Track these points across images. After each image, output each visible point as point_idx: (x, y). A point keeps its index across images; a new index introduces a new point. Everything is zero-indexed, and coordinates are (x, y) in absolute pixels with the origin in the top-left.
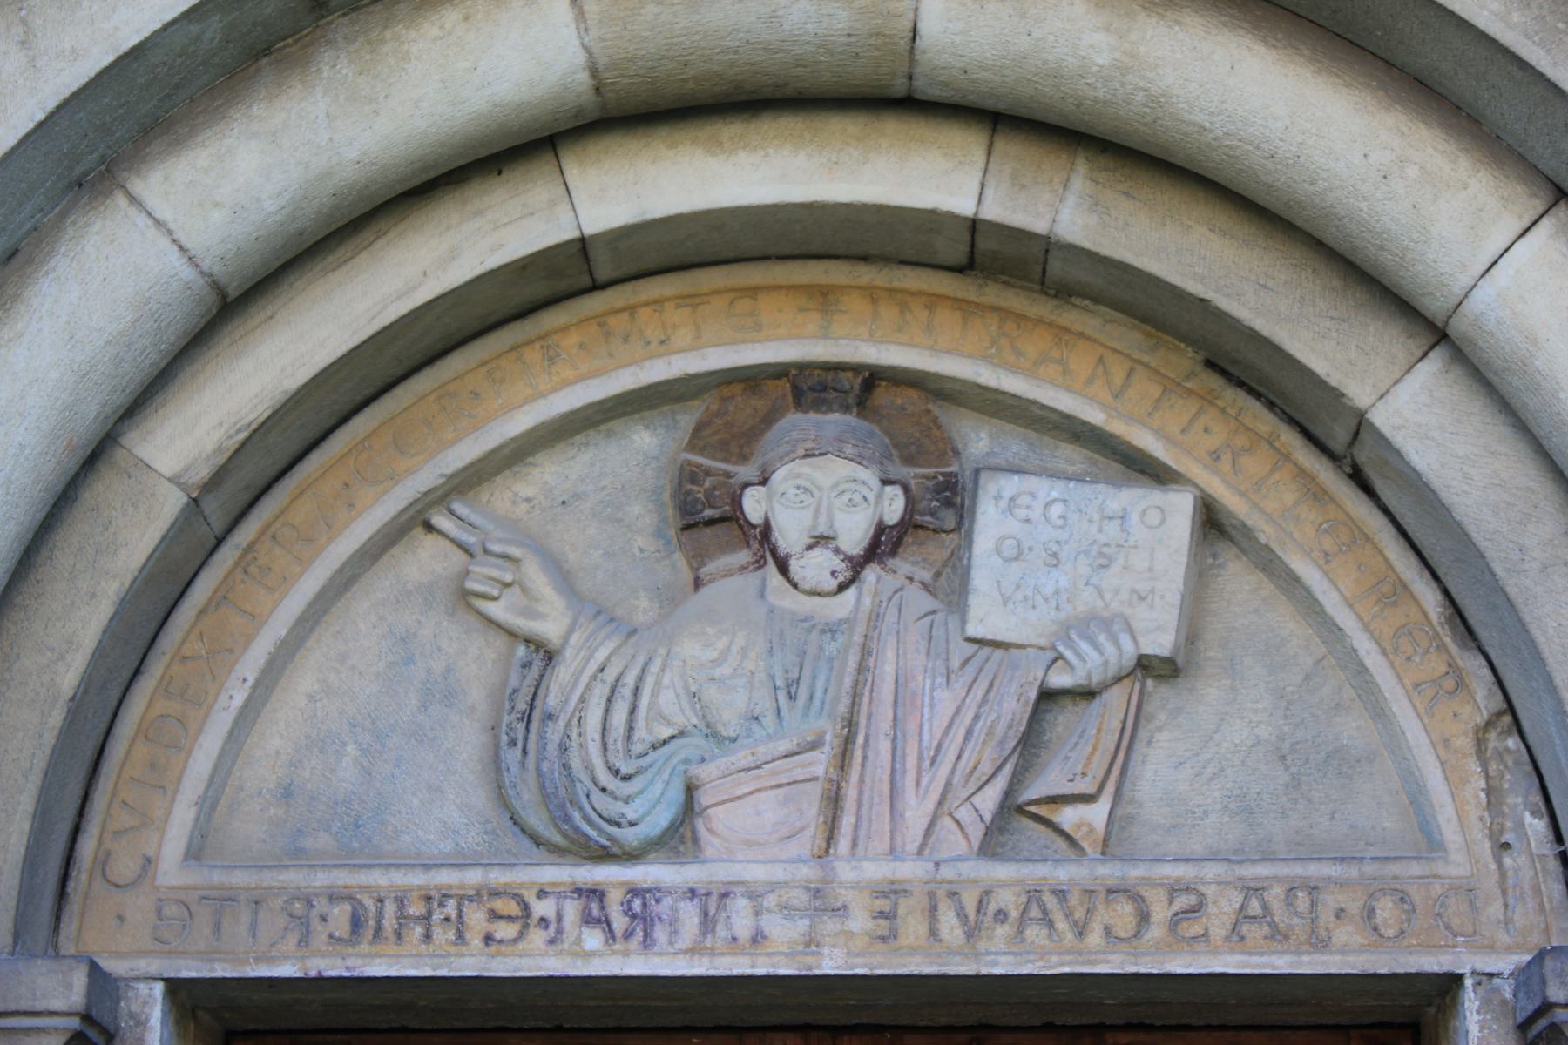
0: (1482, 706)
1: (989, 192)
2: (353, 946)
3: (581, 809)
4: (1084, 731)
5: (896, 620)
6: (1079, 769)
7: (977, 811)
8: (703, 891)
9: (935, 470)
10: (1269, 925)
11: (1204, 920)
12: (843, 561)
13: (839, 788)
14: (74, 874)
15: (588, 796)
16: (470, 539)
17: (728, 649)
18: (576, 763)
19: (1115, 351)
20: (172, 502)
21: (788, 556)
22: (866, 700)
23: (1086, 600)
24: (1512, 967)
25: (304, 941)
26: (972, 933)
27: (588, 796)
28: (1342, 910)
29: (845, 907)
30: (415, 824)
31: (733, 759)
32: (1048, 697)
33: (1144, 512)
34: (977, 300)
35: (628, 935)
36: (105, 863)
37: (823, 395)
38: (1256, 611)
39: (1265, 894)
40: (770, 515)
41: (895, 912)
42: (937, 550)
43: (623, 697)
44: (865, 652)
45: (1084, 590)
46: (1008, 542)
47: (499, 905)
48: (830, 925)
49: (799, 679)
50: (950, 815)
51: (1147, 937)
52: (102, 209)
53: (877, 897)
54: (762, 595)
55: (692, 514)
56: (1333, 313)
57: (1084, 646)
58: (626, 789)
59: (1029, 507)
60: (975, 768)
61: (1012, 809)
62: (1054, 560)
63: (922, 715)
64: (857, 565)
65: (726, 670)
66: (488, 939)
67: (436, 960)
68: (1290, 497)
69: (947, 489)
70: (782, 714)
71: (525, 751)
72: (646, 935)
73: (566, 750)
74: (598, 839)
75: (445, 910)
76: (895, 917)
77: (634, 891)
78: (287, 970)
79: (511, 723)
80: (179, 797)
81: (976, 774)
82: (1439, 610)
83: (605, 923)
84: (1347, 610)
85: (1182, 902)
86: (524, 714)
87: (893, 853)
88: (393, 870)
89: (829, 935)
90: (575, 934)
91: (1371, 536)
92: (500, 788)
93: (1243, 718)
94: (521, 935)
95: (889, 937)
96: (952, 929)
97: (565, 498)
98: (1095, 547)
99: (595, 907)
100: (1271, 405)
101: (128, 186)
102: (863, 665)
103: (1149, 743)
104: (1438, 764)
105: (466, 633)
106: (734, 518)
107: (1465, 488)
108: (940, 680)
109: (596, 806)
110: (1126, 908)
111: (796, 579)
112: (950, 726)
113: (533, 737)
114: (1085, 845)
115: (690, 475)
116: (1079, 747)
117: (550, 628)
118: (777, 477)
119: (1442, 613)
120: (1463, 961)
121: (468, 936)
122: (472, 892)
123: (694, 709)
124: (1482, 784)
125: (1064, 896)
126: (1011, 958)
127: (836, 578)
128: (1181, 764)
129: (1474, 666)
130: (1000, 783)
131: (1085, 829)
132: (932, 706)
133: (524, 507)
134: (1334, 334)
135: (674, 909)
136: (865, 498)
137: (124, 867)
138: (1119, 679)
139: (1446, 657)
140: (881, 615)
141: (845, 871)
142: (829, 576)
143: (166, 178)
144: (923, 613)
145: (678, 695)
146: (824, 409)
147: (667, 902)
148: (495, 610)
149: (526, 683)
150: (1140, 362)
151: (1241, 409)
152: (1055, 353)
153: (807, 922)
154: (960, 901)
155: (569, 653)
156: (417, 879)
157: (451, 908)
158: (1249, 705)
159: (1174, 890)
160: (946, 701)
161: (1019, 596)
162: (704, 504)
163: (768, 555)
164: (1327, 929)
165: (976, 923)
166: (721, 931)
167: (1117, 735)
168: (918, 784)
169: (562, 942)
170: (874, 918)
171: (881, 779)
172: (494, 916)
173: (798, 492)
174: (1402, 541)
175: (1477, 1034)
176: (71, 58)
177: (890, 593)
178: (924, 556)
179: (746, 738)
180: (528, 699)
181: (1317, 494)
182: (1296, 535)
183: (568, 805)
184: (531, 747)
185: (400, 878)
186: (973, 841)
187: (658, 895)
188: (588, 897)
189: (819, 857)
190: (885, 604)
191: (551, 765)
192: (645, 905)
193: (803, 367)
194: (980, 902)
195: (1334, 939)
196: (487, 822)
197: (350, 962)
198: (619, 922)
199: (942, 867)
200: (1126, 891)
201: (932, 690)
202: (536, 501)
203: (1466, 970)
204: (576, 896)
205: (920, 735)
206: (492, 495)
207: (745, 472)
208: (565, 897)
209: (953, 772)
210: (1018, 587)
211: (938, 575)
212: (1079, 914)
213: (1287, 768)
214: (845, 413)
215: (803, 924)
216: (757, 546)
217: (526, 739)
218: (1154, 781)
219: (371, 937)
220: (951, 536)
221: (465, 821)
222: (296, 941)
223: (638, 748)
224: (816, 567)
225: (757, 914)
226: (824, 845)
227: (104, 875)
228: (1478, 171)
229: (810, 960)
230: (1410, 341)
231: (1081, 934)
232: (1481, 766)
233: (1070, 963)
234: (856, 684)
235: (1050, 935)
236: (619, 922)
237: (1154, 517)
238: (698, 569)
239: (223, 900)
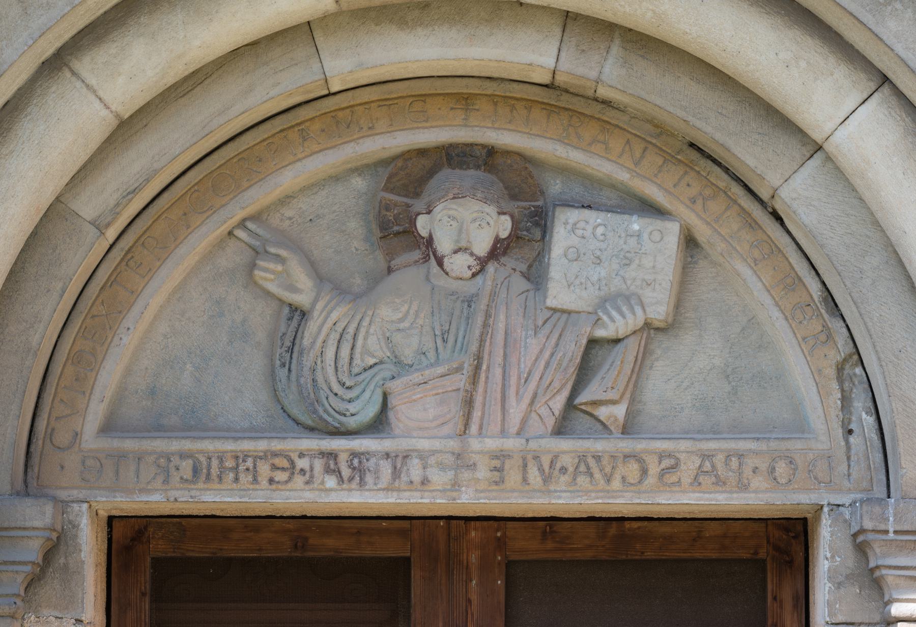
0: (841, 350)
1: (563, 54)
2: (194, 484)
3: (323, 405)
4: (613, 362)
5: (505, 296)
6: (610, 385)
7: (551, 409)
8: (394, 454)
9: (530, 203)
10: (716, 477)
11: (679, 473)
12: (475, 260)
13: (471, 395)
14: (34, 441)
15: (327, 398)
17: (408, 312)
19: (636, 135)
21: (443, 257)
22: (488, 344)
23: (616, 285)
24: (851, 501)
25: (166, 481)
26: (547, 479)
27: (327, 398)
28: (757, 468)
29: (475, 464)
30: (227, 411)
31: (410, 377)
32: (593, 343)
33: (651, 233)
34: (556, 104)
35: (351, 479)
36: (51, 435)
37: (464, 159)
38: (715, 290)
39: (714, 459)
40: (432, 232)
41: (503, 467)
43: (347, 340)
44: (488, 315)
45: (615, 279)
46: (571, 250)
48: (466, 475)
49: (449, 330)
50: (535, 411)
51: (646, 482)
52: (56, 78)
53: (493, 459)
54: (428, 279)
55: (386, 229)
56: (760, 130)
57: (614, 313)
59: (584, 229)
60: (550, 384)
61: (570, 405)
62: (598, 261)
63: (520, 353)
65: (406, 324)
66: (271, 481)
67: (242, 493)
68: (735, 226)
69: (536, 216)
70: (439, 351)
71: (290, 370)
72: (361, 479)
73: (314, 370)
74: (333, 423)
75: (246, 464)
76: (503, 470)
77: (354, 454)
79: (282, 354)
80: (93, 397)
81: (551, 388)
82: (819, 293)
83: (338, 473)
84: (766, 293)
85: (666, 463)
86: (289, 348)
87: (503, 433)
88: (216, 440)
89: (465, 481)
90: (321, 479)
91: (782, 249)
92: (275, 391)
93: (705, 353)
94: (290, 479)
95: (499, 482)
96: (535, 477)
97: (310, 218)
98: (622, 253)
99: (332, 463)
100: (727, 170)
101: (71, 64)
102: (486, 322)
103: (651, 368)
104: (814, 384)
105: (254, 299)
107: (832, 235)
108: (531, 332)
109: (332, 404)
111: (448, 270)
112: (536, 360)
113: (294, 361)
114: (612, 428)
116: (610, 372)
117: (302, 299)
118: (439, 210)
119: (821, 296)
120: (825, 498)
121: (259, 479)
122: (262, 454)
123: (388, 348)
124: (839, 396)
125: (600, 459)
126: (569, 494)
127: (471, 270)
128: (669, 380)
129: (836, 325)
130: (566, 393)
131: (612, 419)
132: (526, 347)
133: (288, 222)
134: (760, 143)
135: (377, 465)
136: (488, 223)
137: (63, 438)
138: (634, 332)
139: (822, 321)
140: (497, 292)
141: (475, 444)
142: (467, 269)
143: (92, 60)
144: (521, 291)
145: (379, 339)
146: (464, 167)
147: (373, 461)
149: (290, 330)
150: (651, 143)
151: (709, 172)
152: (600, 137)
153: (453, 472)
154: (540, 462)
155: (316, 314)
156: (230, 446)
157: (249, 463)
158: (710, 346)
159: (661, 456)
160: (534, 345)
161: (577, 282)
162: (393, 223)
163: (431, 253)
164: (748, 479)
165: (549, 474)
166: (404, 478)
167: (632, 365)
168: (517, 393)
169: (313, 483)
170: (491, 471)
171: (496, 391)
172: (274, 468)
173: (449, 220)
174: (799, 252)
175: (829, 538)
176: (47, 8)
177: (502, 280)
178: (522, 255)
179: (418, 365)
180: (292, 339)
181: (752, 224)
182: (738, 248)
183: (316, 403)
184: (293, 367)
186: (548, 427)
187: (368, 456)
188: (328, 457)
189: (460, 435)
190: (499, 286)
191: (306, 380)
192: (360, 462)
194: (552, 462)
195: (751, 485)
196: (268, 410)
197: (193, 493)
198: (346, 472)
199: (530, 442)
200: (635, 456)
201: (526, 338)
202: (295, 219)
203: (825, 503)
204: (321, 456)
205: (519, 365)
206: (269, 215)
207: (419, 205)
208: (315, 457)
209: (538, 387)
210: (577, 277)
211: (530, 266)
212: (608, 469)
213: (730, 383)
214: (477, 170)
215: (450, 474)
216: (424, 249)
217: (290, 363)
218: (653, 390)
219: (204, 479)
220: (538, 243)
221: (256, 409)
222: (161, 481)
223: (356, 370)
224: (460, 264)
225: (424, 468)
226: (463, 429)
227: (51, 442)
228: (840, 65)
229: (455, 494)
230: (803, 148)
231: (608, 481)
232: (839, 385)
233: (602, 498)
234: (482, 335)
235: (591, 481)
236: (346, 472)
237: (656, 236)
238: (390, 262)
239: (120, 457)
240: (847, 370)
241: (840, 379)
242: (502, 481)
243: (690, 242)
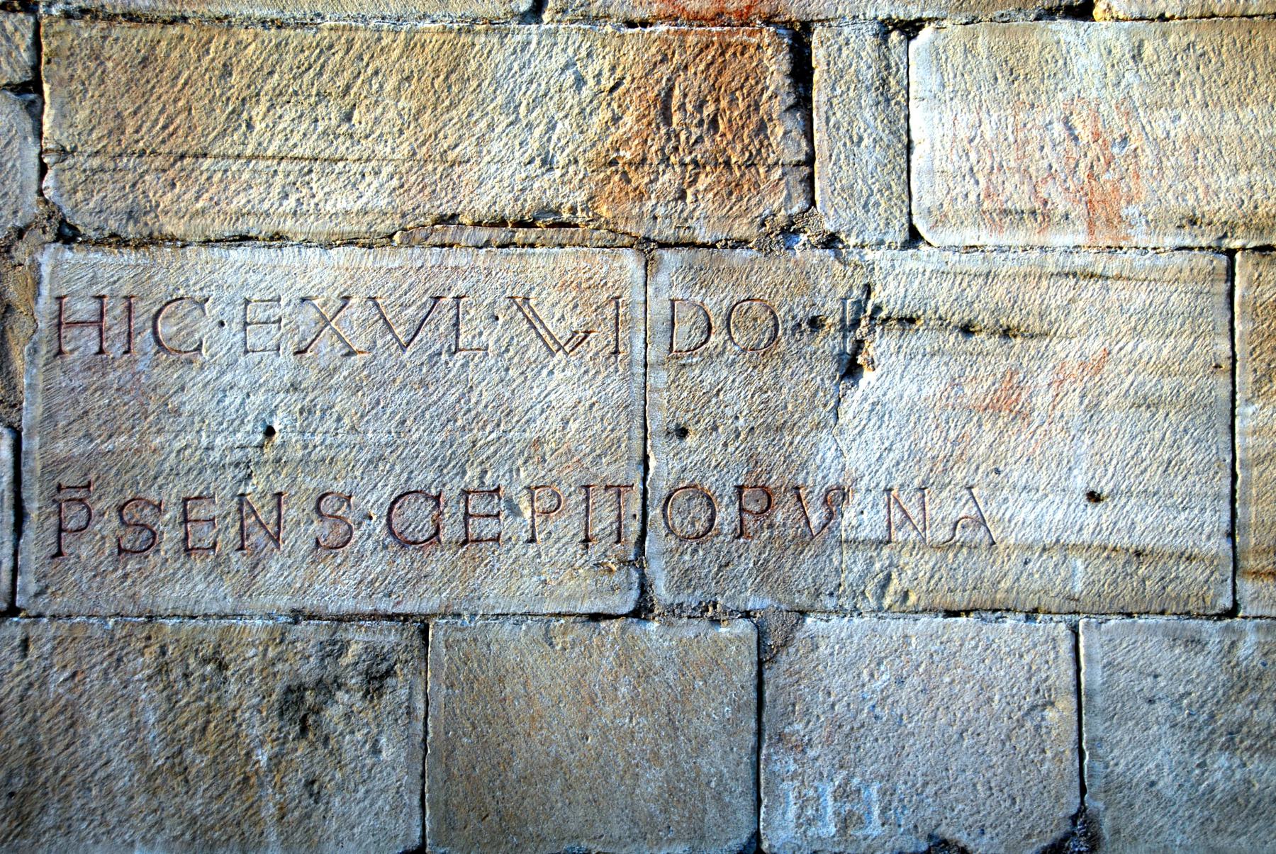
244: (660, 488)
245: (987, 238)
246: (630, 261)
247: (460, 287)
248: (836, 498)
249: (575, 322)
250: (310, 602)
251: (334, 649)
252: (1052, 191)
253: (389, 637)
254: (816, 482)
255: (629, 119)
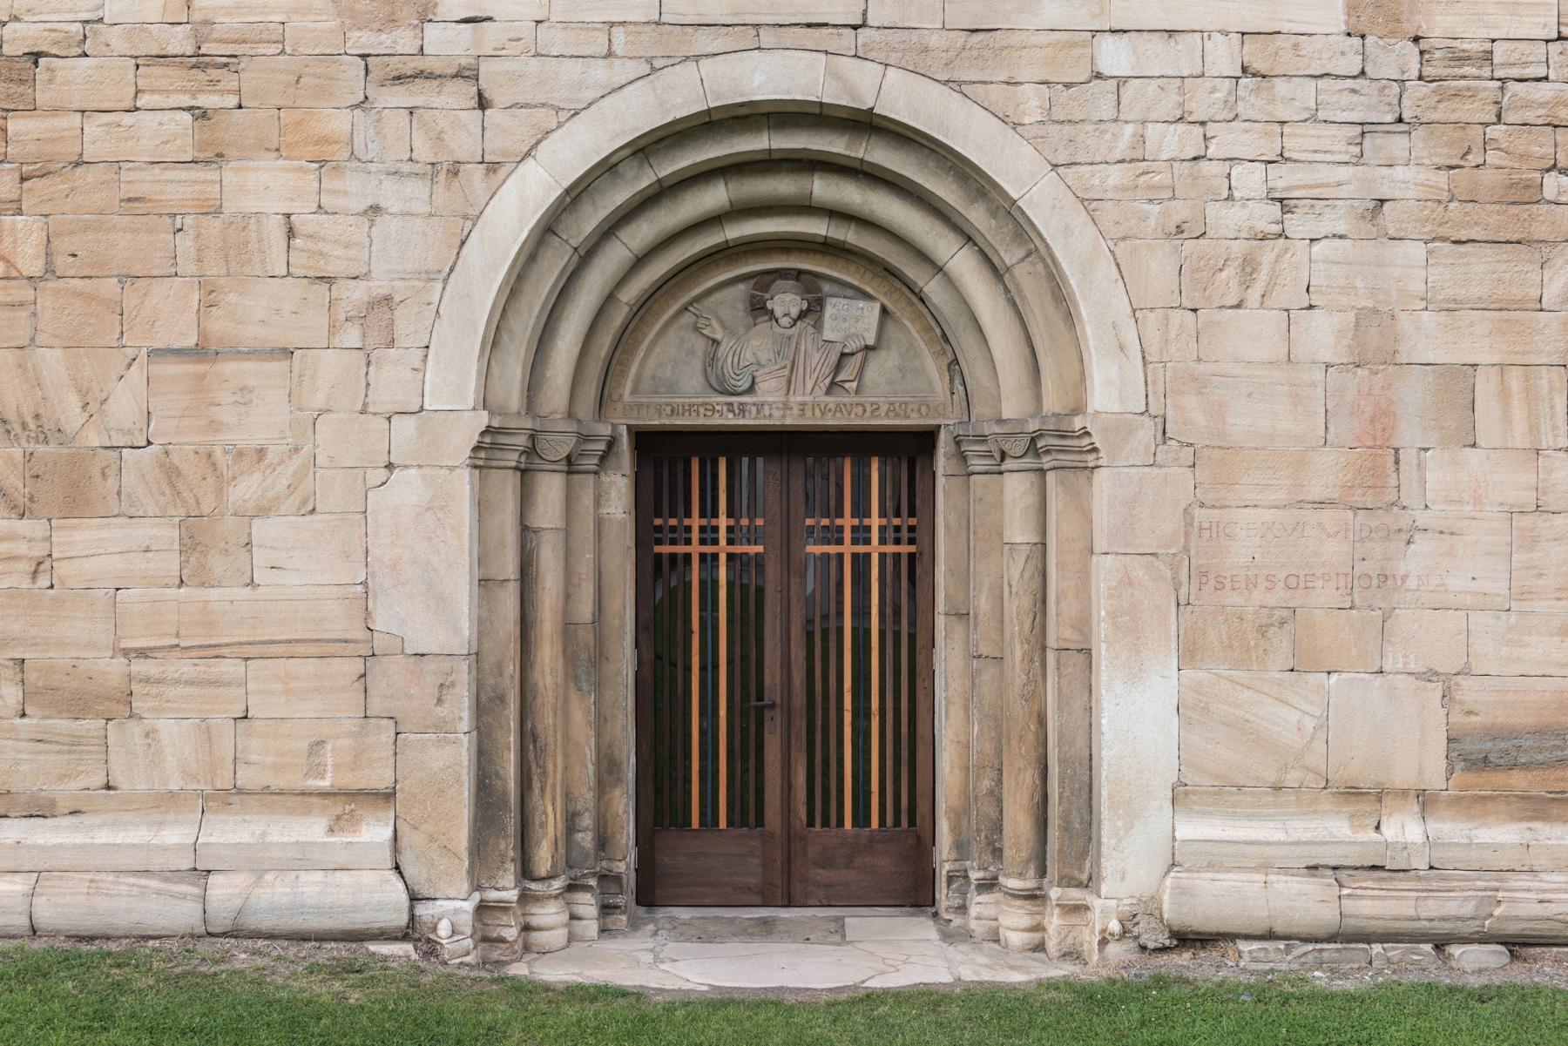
16: (698, 313)
18: (725, 371)
20: (626, 309)
23: (853, 330)
25: (660, 415)
26: (823, 414)
32: (843, 355)
42: (815, 316)
44: (797, 344)
47: (707, 407)
48: (788, 412)
58: (738, 378)
61: (833, 383)
62: (845, 320)
64: (795, 321)
66: (705, 415)
77: (740, 404)
78: (656, 422)
83: (733, 411)
85: (874, 407)
100: (900, 280)
106: (764, 308)
110: (861, 408)
115: (753, 296)
117: (718, 336)
120: (942, 422)
129: (947, 347)
130: (831, 376)
137: (615, 397)
141: (792, 399)
148: (704, 331)
156: (687, 400)
160: (817, 356)
181: (911, 303)
185: (683, 400)
191: (719, 372)
193: (782, 269)
198: (737, 411)
207: (767, 296)
236: (737, 411)
239: (639, 405)
240: (952, 366)
241: (949, 370)
242: (804, 414)
243: (884, 311)
244: (1357, 575)
245: (1446, 507)
246: (1350, 514)
247: (1305, 520)
248: (1404, 578)
249: (1335, 529)
250: (1264, 604)
251: (1271, 616)
252: (1464, 495)
253: (1285, 613)
254: (1400, 574)
255: (1350, 475)
